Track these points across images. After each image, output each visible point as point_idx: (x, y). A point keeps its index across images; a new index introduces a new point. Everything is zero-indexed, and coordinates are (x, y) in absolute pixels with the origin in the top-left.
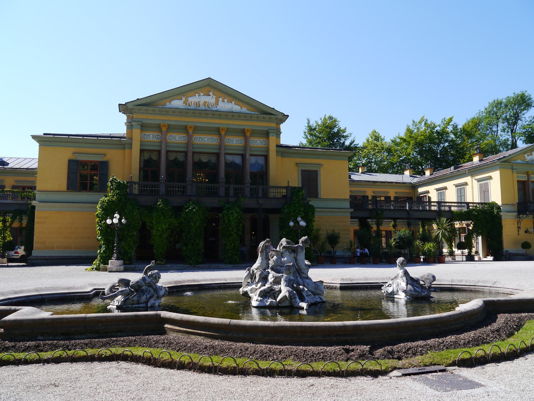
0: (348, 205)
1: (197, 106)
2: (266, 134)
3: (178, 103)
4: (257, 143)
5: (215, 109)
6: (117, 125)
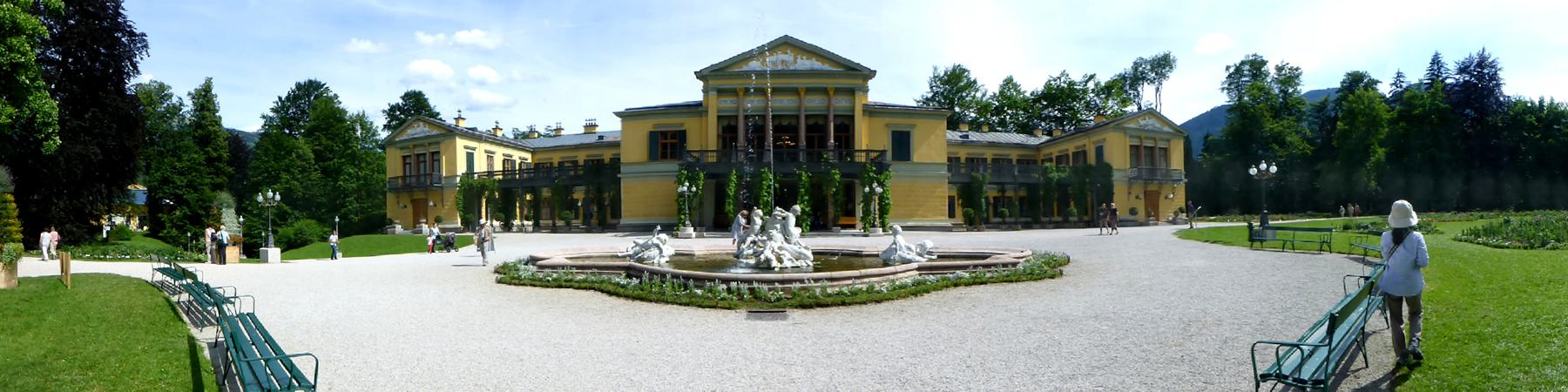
2: (851, 92)
3: (755, 65)
4: (841, 103)
6: (693, 92)
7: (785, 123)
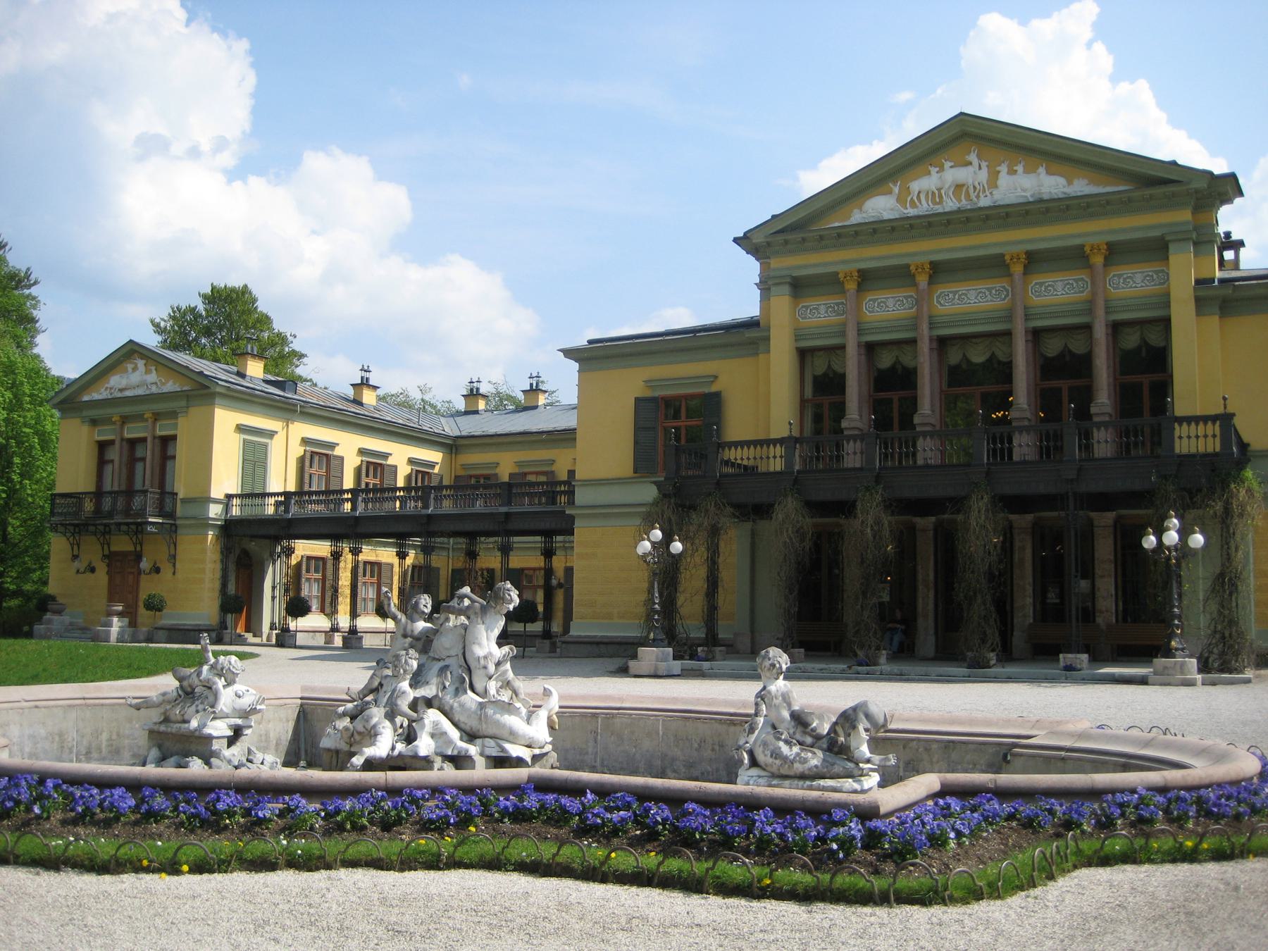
1: (935, 203)
3: (881, 206)
4: (1130, 285)
5: (984, 202)
6: (735, 292)
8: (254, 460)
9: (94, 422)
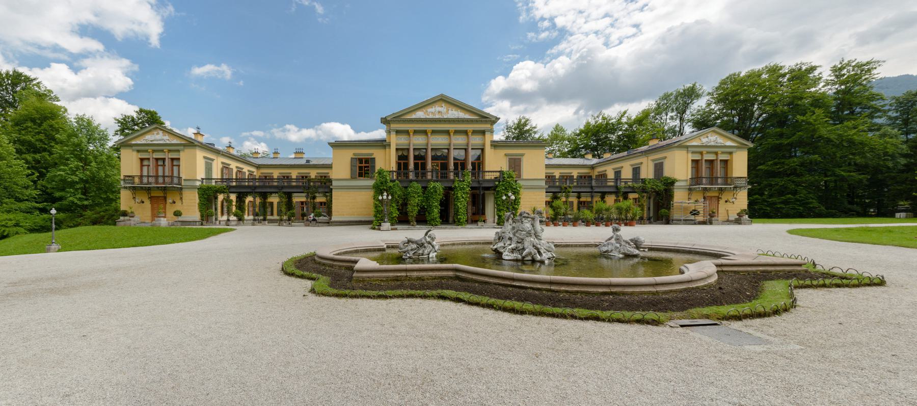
0: (543, 183)
2: (483, 133)
3: (420, 114)
7: (439, 154)
8: (209, 168)
9: (138, 151)
